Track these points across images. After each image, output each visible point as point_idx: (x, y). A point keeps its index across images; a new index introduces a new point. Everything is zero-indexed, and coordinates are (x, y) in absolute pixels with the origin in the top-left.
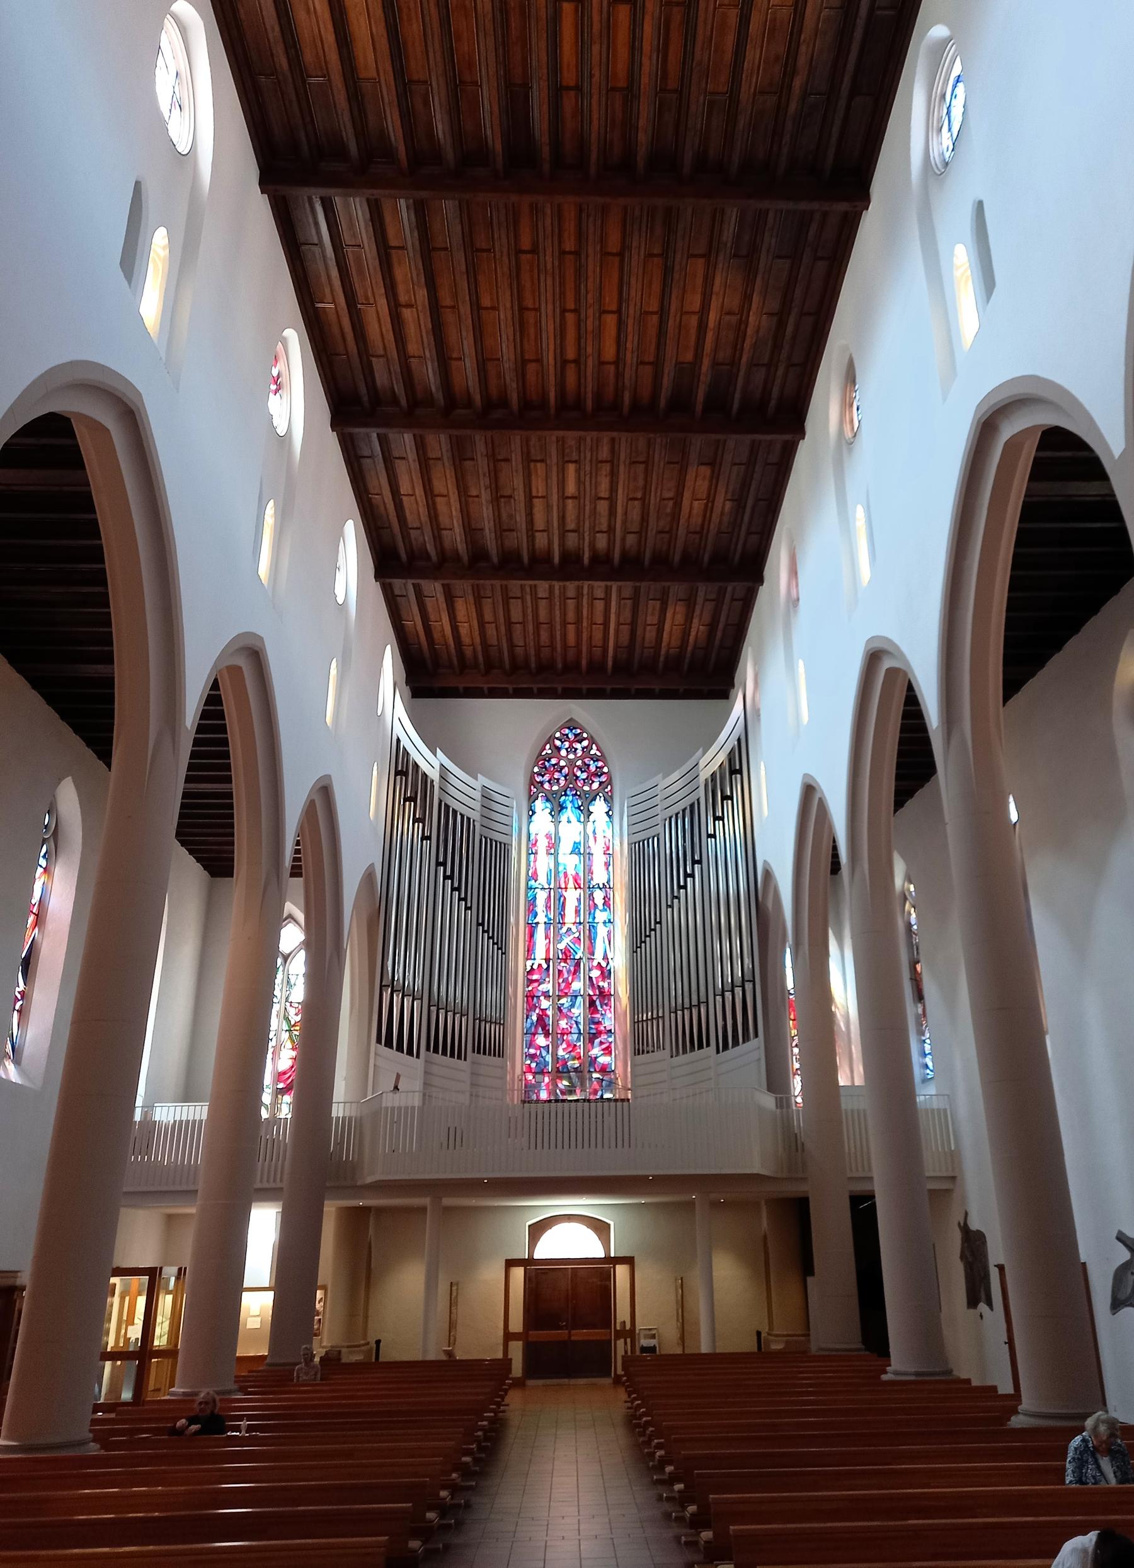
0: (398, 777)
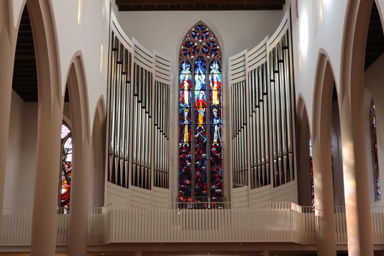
0: (113, 52)
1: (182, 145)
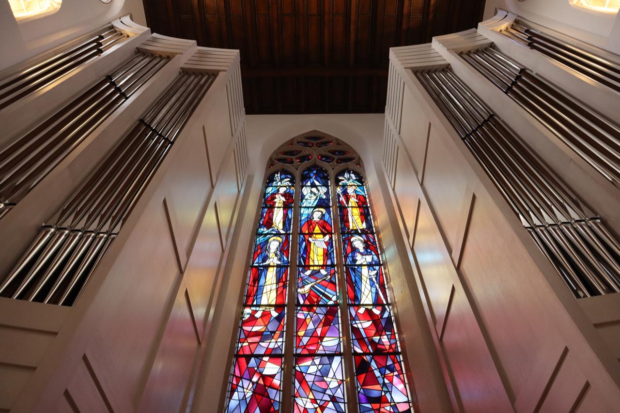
1: (256, 311)
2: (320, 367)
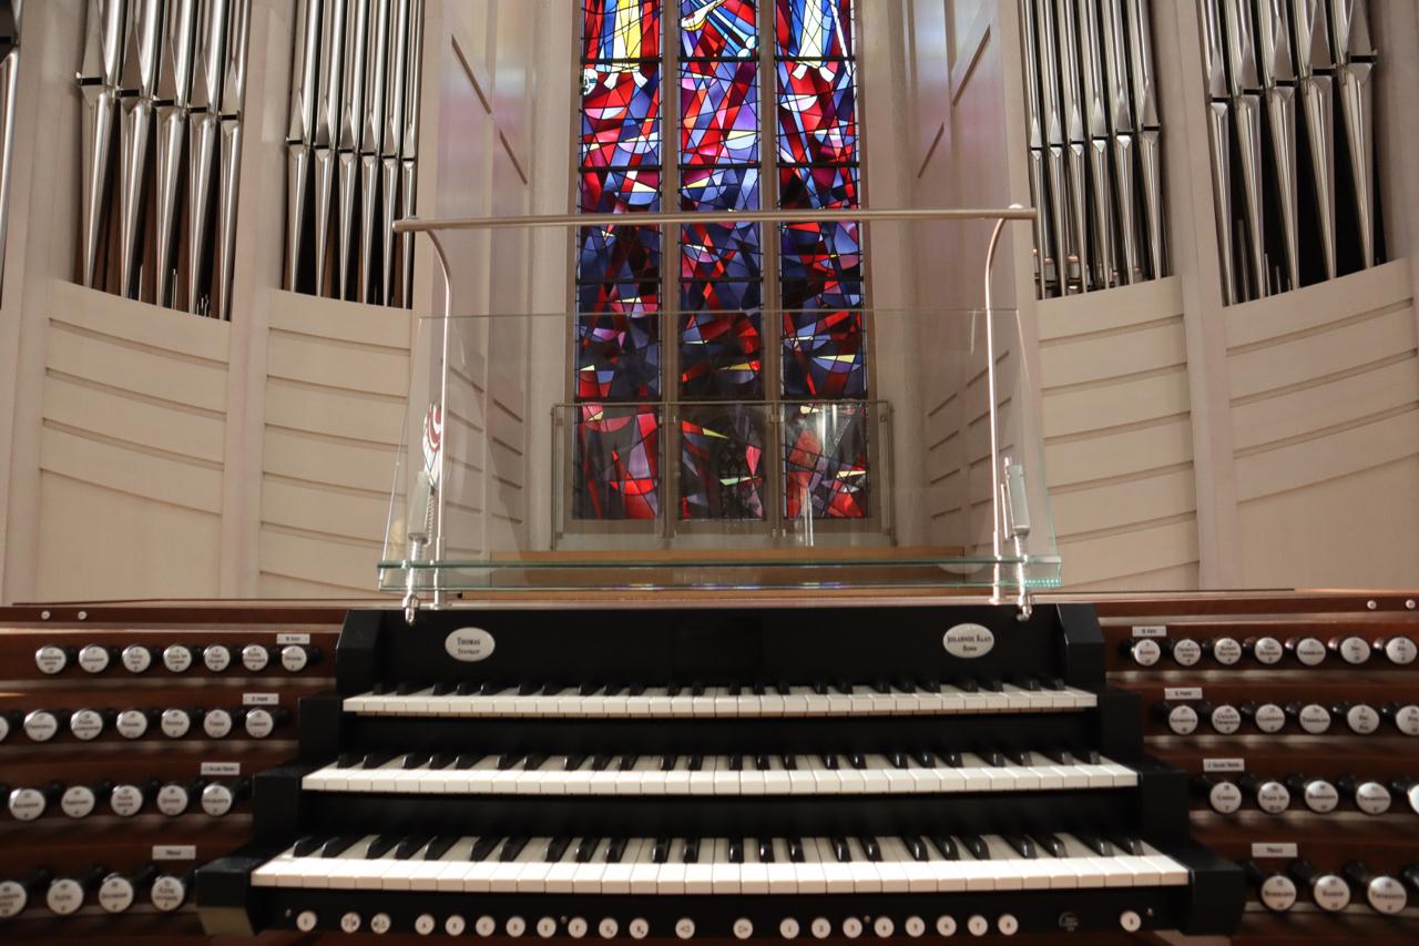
1: (604, 76)
2: (723, 189)
